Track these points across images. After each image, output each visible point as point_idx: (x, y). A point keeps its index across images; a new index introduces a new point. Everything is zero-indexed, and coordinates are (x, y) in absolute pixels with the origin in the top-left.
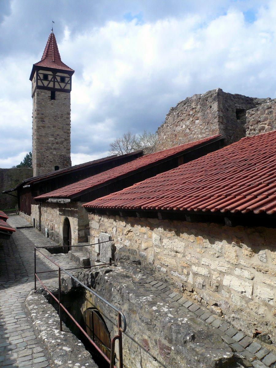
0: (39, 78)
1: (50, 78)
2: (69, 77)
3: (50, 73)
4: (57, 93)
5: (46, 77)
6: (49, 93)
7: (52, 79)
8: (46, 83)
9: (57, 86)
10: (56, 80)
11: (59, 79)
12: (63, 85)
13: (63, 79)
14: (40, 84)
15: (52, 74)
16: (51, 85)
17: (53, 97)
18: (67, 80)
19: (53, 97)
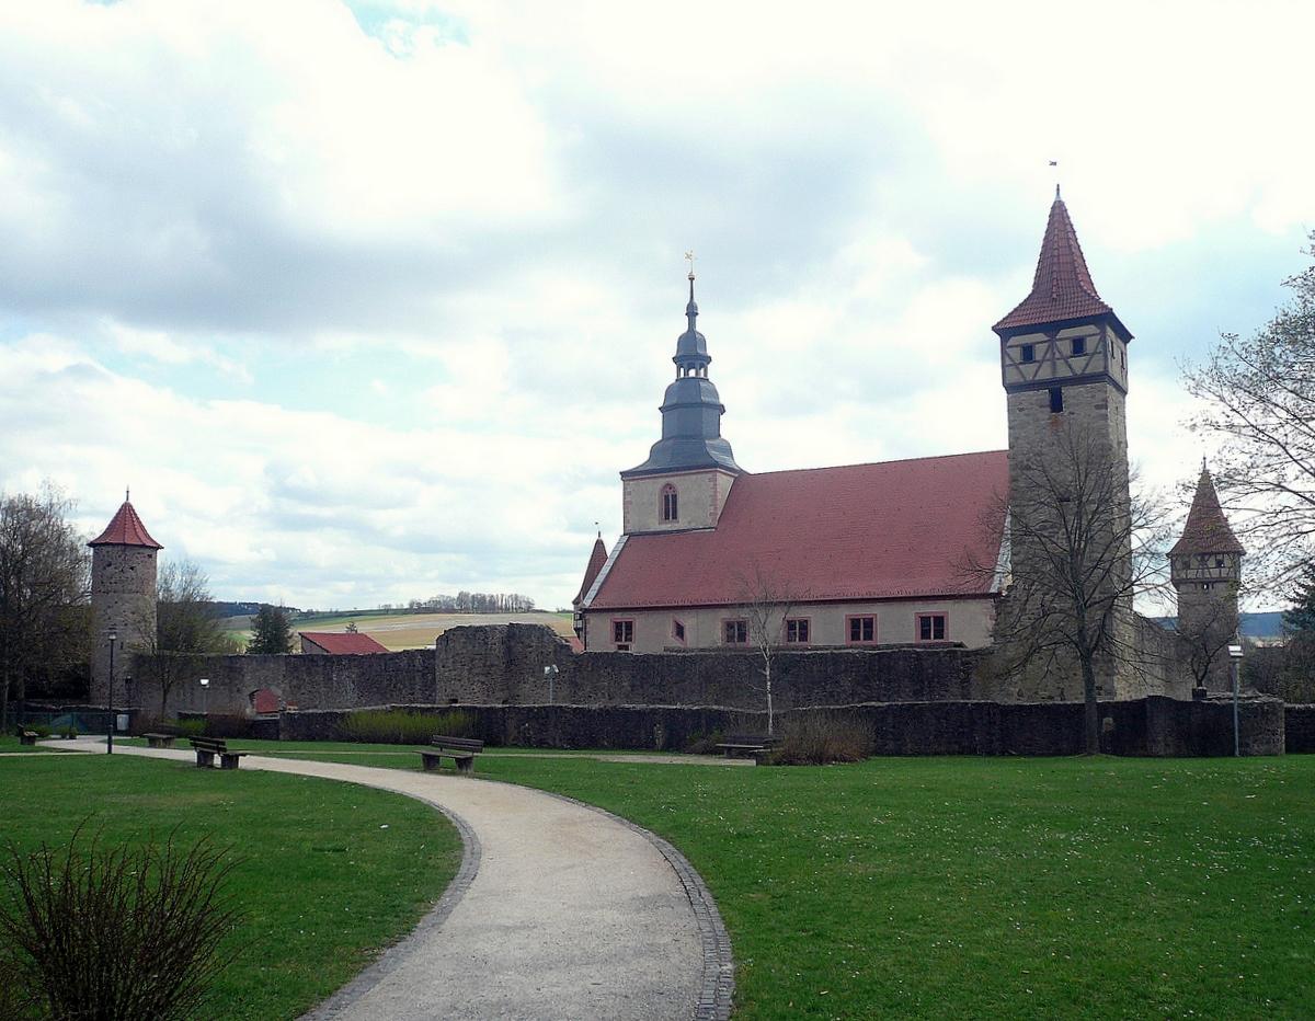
0: (1008, 362)
1: (1039, 353)
2: (1098, 331)
3: (1040, 337)
4: (1067, 392)
5: (1028, 353)
6: (1044, 395)
7: (1046, 354)
8: (1029, 370)
9: (1063, 372)
10: (1057, 355)
11: (1066, 348)
12: (1078, 363)
13: (1078, 346)
14: (1014, 377)
15: (1046, 339)
16: (1045, 373)
17: (1056, 404)
18: (1090, 345)
19: (1056, 404)
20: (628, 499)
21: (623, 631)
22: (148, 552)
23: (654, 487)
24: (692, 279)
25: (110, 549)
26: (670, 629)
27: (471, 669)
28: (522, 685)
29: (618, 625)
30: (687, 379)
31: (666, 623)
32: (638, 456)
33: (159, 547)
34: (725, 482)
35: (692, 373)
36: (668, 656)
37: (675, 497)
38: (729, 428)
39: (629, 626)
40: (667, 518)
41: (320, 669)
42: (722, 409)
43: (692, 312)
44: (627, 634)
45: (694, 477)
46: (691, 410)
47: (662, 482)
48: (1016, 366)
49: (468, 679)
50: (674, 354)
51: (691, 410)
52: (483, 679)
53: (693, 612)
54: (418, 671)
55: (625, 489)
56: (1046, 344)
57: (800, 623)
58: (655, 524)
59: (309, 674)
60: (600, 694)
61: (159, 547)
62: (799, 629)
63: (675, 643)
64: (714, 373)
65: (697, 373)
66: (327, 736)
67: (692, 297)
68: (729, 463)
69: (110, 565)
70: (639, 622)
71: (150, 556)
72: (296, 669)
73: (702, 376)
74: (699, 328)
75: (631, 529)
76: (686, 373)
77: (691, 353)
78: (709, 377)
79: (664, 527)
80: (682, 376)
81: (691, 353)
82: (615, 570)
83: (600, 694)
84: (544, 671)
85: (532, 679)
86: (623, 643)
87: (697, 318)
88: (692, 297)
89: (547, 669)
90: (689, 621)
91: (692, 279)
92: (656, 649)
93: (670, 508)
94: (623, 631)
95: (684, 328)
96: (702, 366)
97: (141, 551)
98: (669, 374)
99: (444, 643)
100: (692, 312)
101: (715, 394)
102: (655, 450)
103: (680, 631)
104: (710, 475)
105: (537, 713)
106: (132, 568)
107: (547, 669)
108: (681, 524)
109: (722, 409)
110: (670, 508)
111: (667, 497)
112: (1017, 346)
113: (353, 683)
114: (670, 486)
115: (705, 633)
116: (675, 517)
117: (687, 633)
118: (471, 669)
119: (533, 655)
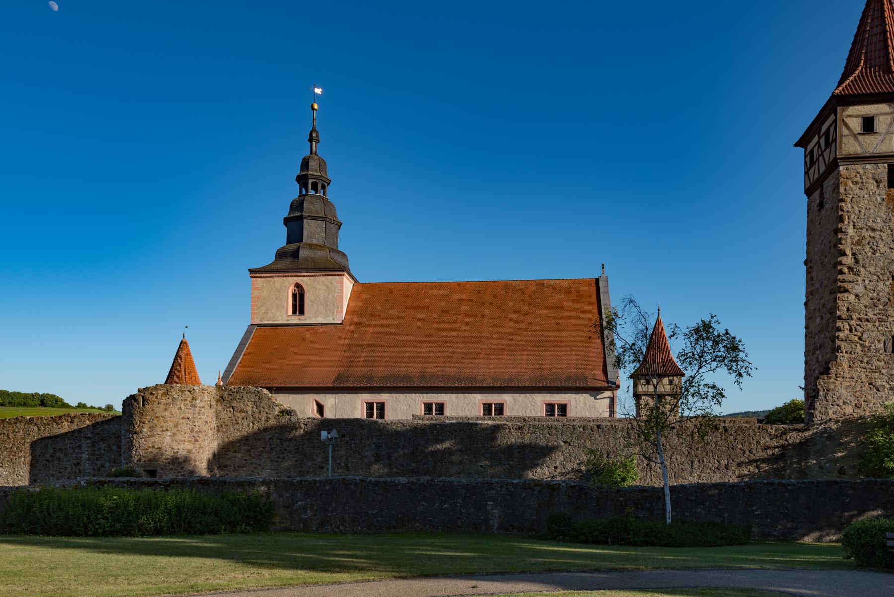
1: (880, 125)
5: (868, 125)
20: (256, 293)
27: (174, 434)
34: (348, 285)
40: (294, 312)
45: (323, 278)
48: (855, 136)
54: (86, 438)
56: (889, 118)
58: (284, 314)
79: (296, 320)
85: (244, 448)
103: (320, 408)
104: (337, 278)
111: (294, 295)
112: (857, 116)
114: (298, 285)
116: (302, 312)
118: (174, 434)
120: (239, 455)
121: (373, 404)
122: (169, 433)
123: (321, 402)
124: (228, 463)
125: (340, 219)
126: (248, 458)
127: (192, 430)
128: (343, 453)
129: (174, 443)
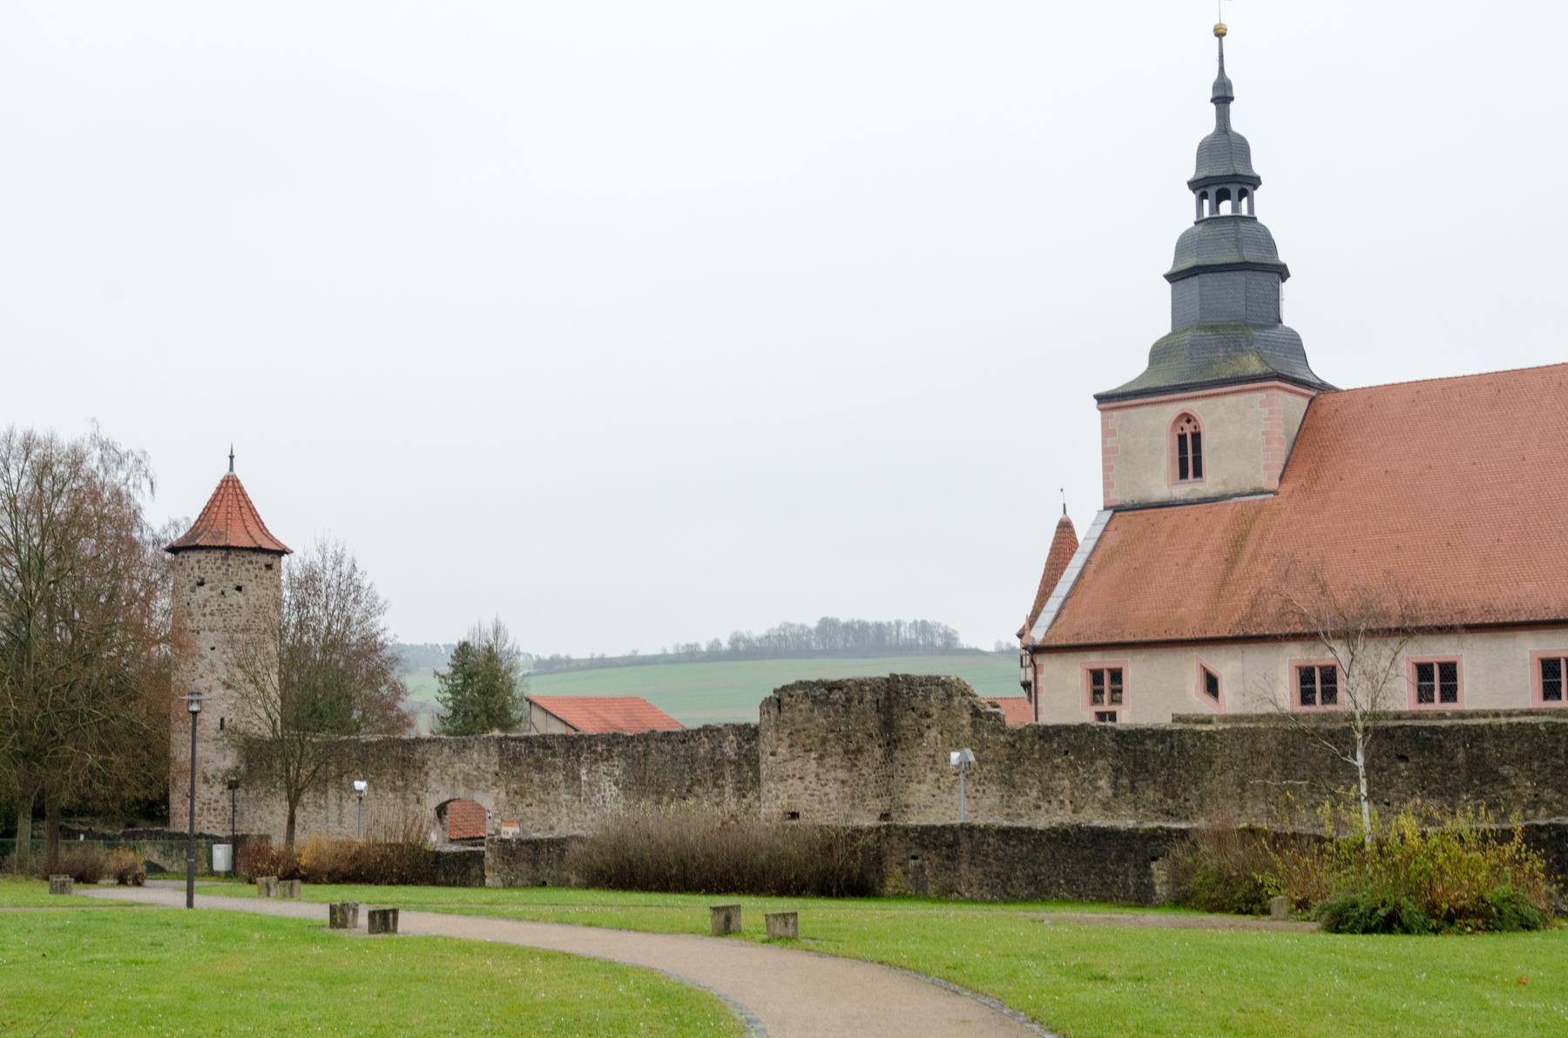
21: (1106, 684)
22: (267, 559)
23: (1160, 420)
24: (1220, 33)
25: (202, 555)
26: (1195, 682)
27: (821, 757)
28: (914, 786)
29: (1097, 676)
30: (1215, 220)
31: (1184, 671)
32: (1131, 367)
33: (282, 552)
34: (1293, 405)
35: (1226, 208)
36: (1180, 732)
37: (1197, 437)
38: (1297, 307)
39: (1117, 675)
40: (1183, 474)
41: (559, 762)
42: (1282, 272)
43: (1222, 97)
44: (1114, 691)
45: (1231, 400)
46: (1229, 278)
47: (1174, 410)
49: (817, 775)
50: (1190, 172)
51: (1229, 278)
52: (842, 774)
53: (1236, 650)
55: (1104, 424)
57: (1441, 665)
58: (1161, 483)
59: (540, 769)
60: (1055, 803)
61: (282, 552)
62: (1439, 679)
63: (1199, 704)
64: (1266, 206)
65: (1236, 208)
66: (568, 880)
67: (1222, 69)
68: (1301, 374)
69: (201, 584)
70: (1135, 668)
71: (269, 567)
72: (516, 760)
73: (1245, 212)
74: (1236, 125)
75: (1118, 498)
76: (1215, 207)
77: (1225, 176)
78: (1257, 214)
80: (1206, 214)
81: (1225, 176)
82: (1088, 577)
83: (1055, 803)
84: (947, 760)
85: (931, 776)
86: (1106, 707)
87: (1232, 105)
88: (1222, 69)
89: (955, 756)
90: (1227, 665)
91: (1220, 33)
92: (1159, 717)
93: (1189, 454)
94: (1106, 684)
95: (1209, 126)
96: (1243, 193)
97: (254, 558)
98: (1184, 211)
99: (774, 711)
100: (1222, 97)
101: (1268, 244)
102: (1160, 353)
104: (1262, 395)
105: (936, 838)
106: (239, 589)
107: (955, 756)
108: (1209, 484)
109: (1282, 272)
110: (1189, 454)
111: (1182, 438)
113: (616, 784)
115: (1261, 685)
116: (1198, 473)
117: (1223, 687)
119: (933, 733)
120: (924, 787)
121: (1312, 669)
122: (813, 755)
123: (1214, 669)
124: (911, 800)
125: (1283, 258)
126: (936, 791)
127: (846, 752)
128: (1066, 782)
129: (821, 771)
